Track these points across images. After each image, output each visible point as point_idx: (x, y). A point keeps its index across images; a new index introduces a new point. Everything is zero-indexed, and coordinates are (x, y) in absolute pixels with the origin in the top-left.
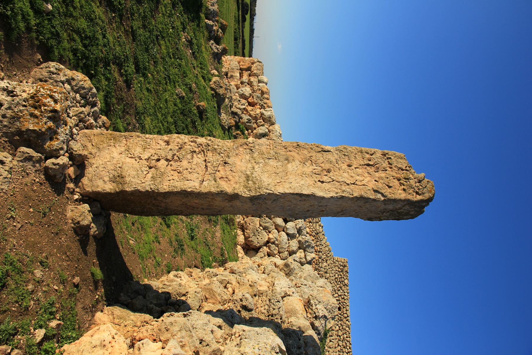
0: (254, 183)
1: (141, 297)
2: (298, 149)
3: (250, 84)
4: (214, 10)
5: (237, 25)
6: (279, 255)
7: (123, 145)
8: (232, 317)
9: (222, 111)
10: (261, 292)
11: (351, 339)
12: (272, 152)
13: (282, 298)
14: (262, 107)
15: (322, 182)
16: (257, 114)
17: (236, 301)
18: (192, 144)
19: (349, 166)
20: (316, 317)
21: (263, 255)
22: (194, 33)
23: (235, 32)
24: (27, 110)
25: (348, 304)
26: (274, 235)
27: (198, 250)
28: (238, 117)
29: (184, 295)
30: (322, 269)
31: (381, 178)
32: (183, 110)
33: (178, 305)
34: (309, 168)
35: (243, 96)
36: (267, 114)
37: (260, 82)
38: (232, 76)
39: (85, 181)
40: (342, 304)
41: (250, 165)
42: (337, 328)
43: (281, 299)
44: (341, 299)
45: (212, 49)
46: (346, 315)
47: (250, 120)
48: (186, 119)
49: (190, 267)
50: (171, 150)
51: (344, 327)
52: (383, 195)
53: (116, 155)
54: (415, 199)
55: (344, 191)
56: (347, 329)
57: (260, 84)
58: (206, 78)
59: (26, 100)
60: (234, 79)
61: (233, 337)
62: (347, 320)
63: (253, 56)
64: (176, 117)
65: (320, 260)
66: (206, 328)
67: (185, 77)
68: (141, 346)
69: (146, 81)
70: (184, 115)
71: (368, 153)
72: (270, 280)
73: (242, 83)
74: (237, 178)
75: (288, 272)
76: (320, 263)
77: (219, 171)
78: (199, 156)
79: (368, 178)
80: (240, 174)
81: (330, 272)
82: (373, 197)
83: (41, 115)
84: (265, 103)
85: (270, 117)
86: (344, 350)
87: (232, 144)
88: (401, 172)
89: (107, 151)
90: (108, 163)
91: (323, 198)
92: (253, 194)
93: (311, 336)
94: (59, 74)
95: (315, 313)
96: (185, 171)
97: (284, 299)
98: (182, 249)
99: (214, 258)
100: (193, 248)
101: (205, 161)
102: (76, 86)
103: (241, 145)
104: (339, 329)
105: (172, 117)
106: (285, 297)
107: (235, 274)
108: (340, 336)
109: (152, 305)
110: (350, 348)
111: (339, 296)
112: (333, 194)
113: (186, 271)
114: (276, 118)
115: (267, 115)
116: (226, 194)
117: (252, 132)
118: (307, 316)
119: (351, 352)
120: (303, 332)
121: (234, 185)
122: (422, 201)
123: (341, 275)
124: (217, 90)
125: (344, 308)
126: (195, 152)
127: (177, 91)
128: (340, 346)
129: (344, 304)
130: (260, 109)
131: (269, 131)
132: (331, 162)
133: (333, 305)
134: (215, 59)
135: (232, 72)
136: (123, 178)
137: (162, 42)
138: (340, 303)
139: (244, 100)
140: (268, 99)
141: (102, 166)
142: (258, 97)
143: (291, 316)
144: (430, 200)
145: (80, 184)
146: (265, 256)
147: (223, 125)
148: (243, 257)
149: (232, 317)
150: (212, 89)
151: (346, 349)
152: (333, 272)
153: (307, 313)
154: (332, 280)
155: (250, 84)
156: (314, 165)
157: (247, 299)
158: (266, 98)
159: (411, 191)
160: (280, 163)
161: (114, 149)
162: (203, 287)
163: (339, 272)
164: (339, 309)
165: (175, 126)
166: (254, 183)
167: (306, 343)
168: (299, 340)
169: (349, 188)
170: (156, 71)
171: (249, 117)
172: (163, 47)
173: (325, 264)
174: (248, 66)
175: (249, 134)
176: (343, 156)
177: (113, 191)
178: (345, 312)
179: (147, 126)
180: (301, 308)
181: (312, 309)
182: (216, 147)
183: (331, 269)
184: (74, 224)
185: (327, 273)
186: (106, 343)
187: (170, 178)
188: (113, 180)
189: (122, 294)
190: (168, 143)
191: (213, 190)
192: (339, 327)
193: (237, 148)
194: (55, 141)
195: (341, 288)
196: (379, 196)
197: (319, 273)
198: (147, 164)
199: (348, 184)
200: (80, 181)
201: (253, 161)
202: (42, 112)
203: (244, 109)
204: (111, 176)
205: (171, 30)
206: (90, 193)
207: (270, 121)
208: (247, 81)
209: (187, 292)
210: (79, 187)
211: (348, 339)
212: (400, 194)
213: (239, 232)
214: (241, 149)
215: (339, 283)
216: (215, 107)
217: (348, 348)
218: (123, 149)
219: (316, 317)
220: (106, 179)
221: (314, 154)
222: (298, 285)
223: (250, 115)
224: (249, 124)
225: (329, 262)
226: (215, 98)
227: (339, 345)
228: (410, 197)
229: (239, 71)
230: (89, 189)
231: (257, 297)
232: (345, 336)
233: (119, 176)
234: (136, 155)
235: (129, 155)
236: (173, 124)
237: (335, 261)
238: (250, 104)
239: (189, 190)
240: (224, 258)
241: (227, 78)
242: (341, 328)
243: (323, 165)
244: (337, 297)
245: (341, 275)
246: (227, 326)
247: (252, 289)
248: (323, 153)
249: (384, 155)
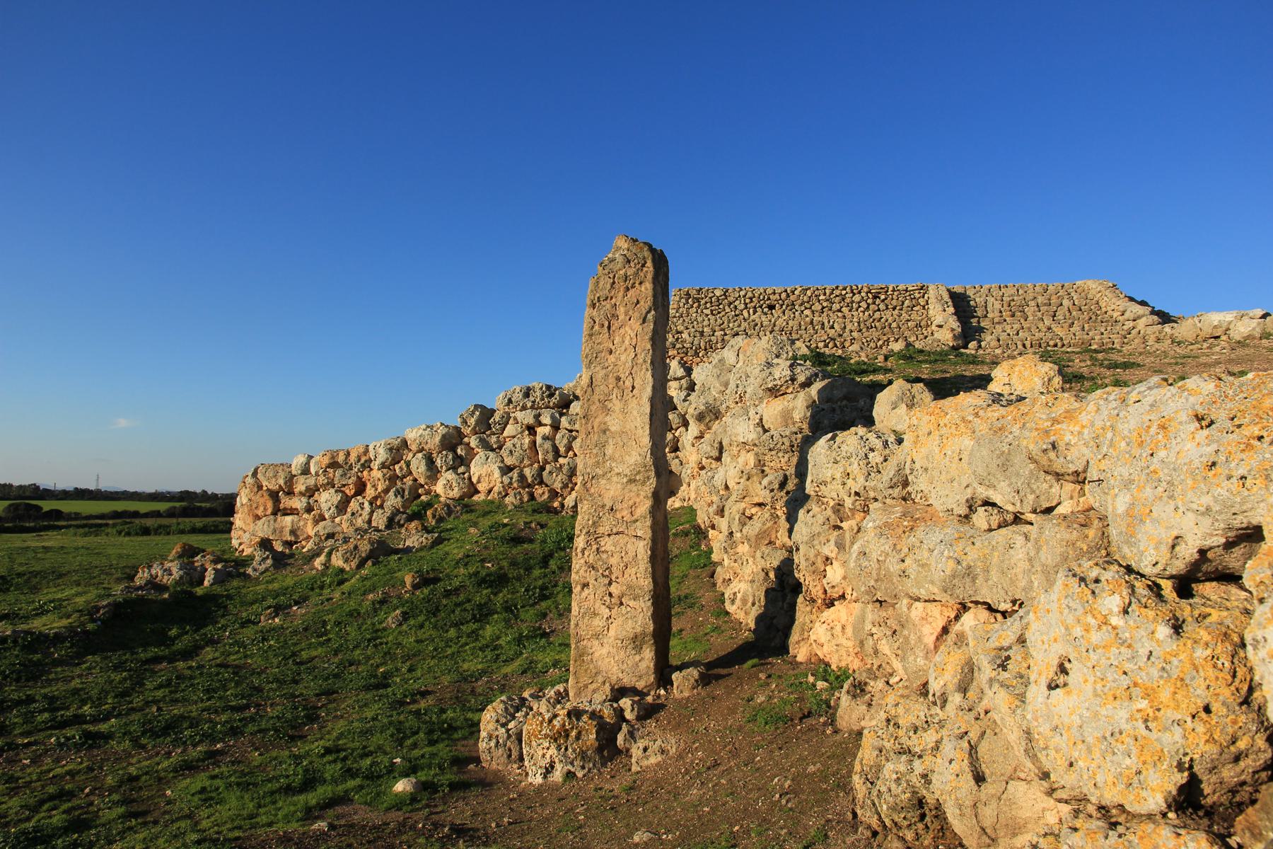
0: (639, 472)
1: (775, 621)
2: (589, 417)
3: (311, 492)
4: (181, 569)
5: (109, 530)
6: (676, 430)
7: (589, 644)
8: (796, 500)
9: (401, 546)
10: (757, 462)
11: (828, 287)
12: (595, 451)
13: (765, 431)
14: (367, 465)
15: (633, 387)
16: (384, 475)
17: (773, 498)
18: (586, 553)
19: (611, 352)
20: (793, 379)
21: (677, 460)
22: (252, 604)
23: (128, 534)
24: (572, 744)
25: (762, 291)
27: (681, 574)
28: (397, 515)
29: (767, 574)
30: (696, 342)
31: (626, 313)
32: (428, 612)
33: (782, 576)
34: (616, 405)
35: (342, 508)
36: (382, 455)
37: (306, 471)
38: (293, 532)
39: (640, 685)
40: (761, 302)
41: (615, 479)
42: (807, 312)
43: (768, 434)
44: (753, 304)
45: (267, 570)
46: (784, 295)
47: (397, 490)
48: (445, 606)
49: (714, 585)
50: (596, 580)
51: (806, 299)
52: (648, 312)
53: (604, 651)
54: (652, 269)
55: (645, 361)
56: (809, 293)
57: (313, 470)
58: (341, 577)
59: (559, 748)
60: (299, 528)
61: (819, 494)
62: (793, 292)
63: (218, 487)
64: (445, 624)
65: (678, 346)
66: (810, 523)
67: (359, 614)
68: (830, 585)
69: (396, 674)
70: (438, 610)
71: (593, 327)
72: (735, 450)
73: (309, 509)
74: (632, 494)
75: (711, 414)
76: (684, 347)
77: (623, 517)
78: (602, 544)
79: (627, 329)
80: (626, 491)
81: (700, 325)
82: (652, 324)
83: (577, 728)
84: (359, 461)
85: (391, 449)
86: (848, 300)
87: (586, 502)
88: (616, 286)
89: (600, 663)
90: (616, 659)
91: (653, 387)
92: (653, 474)
93: (819, 392)
94: (497, 736)
95: (787, 381)
96: (625, 560)
97: (766, 427)
98: (686, 597)
99: (692, 547)
100: (679, 583)
101: (609, 535)
102: (506, 717)
103: (587, 491)
104: (811, 308)
105: (447, 631)
106: (763, 426)
107: (723, 507)
108: (823, 308)
109: (785, 606)
110: (845, 289)
111: (746, 308)
112: (649, 374)
113: (722, 589)
114: (392, 438)
115: (385, 456)
116: (653, 507)
117: (422, 486)
118: (792, 393)
119: (851, 287)
120: (814, 401)
121: (642, 497)
122: (654, 261)
123: (706, 303)
124: (363, 555)
125: (769, 299)
126: (598, 549)
127: (393, 626)
128: (842, 307)
129: (761, 297)
130: (371, 469)
131: (421, 451)
132: (607, 375)
133: (771, 343)
134: (288, 564)
135: (281, 532)
136: (636, 637)
137: (305, 655)
138: (761, 307)
139: (351, 504)
140: (348, 454)
141: (620, 665)
142: (344, 475)
143: (792, 418)
144: (652, 250)
145: (645, 691)
146: (677, 457)
147: (433, 542)
148: (681, 499)
149: (796, 500)
150: (361, 565)
151: (847, 296)
152: (700, 319)
153: (786, 393)
154: (716, 320)
155: (311, 492)
156: (611, 397)
157: (771, 483)
158: (346, 458)
159: (642, 274)
160: (610, 441)
161: (596, 655)
162: (753, 550)
163: (699, 305)
164: (771, 307)
165: (462, 624)
166: (639, 472)
167: (829, 400)
168: (823, 410)
169: (641, 354)
170: (367, 662)
171: (391, 493)
172: (314, 653)
173: (685, 335)
174: (267, 497)
175: (428, 492)
176: (598, 359)
177: (654, 648)
178: (777, 296)
179: (480, 667)
180: (779, 402)
181: (781, 386)
182: (590, 522)
183: (695, 323)
184: (699, 685)
185: (703, 332)
186: (829, 627)
187: (634, 577)
188: (638, 649)
189: (773, 644)
190: (585, 585)
191: (649, 523)
192: (806, 308)
193: (591, 495)
194: (604, 713)
195: (731, 303)
196: (650, 316)
197: (703, 348)
198: (616, 608)
199: (636, 355)
200: (641, 691)
201: (609, 475)
202: (572, 728)
203: (371, 503)
204: (633, 652)
205: (272, 643)
206: (656, 676)
207: (398, 450)
208: (304, 500)
209: (763, 570)
210: (649, 691)
211: (828, 292)
212: (646, 289)
214: (592, 491)
215: (721, 307)
216: (400, 559)
217: (844, 292)
218: (596, 643)
219: (793, 379)
220: (637, 658)
221: (596, 397)
222: (737, 400)
223: (386, 491)
224: (406, 493)
225: (680, 328)
226: (380, 560)
227: (839, 311)
228: (650, 276)
229: (279, 518)
230: (652, 678)
231: (765, 468)
232: (822, 297)
233: (634, 642)
234: (605, 624)
235: (605, 632)
236: (460, 629)
237: (677, 315)
238: (361, 488)
239: (649, 552)
240: (692, 531)
241: (296, 543)
242: (808, 306)
243: (611, 386)
244: (749, 312)
245: (706, 303)
246: (807, 504)
247: (753, 476)
248: (594, 385)
249: (594, 306)
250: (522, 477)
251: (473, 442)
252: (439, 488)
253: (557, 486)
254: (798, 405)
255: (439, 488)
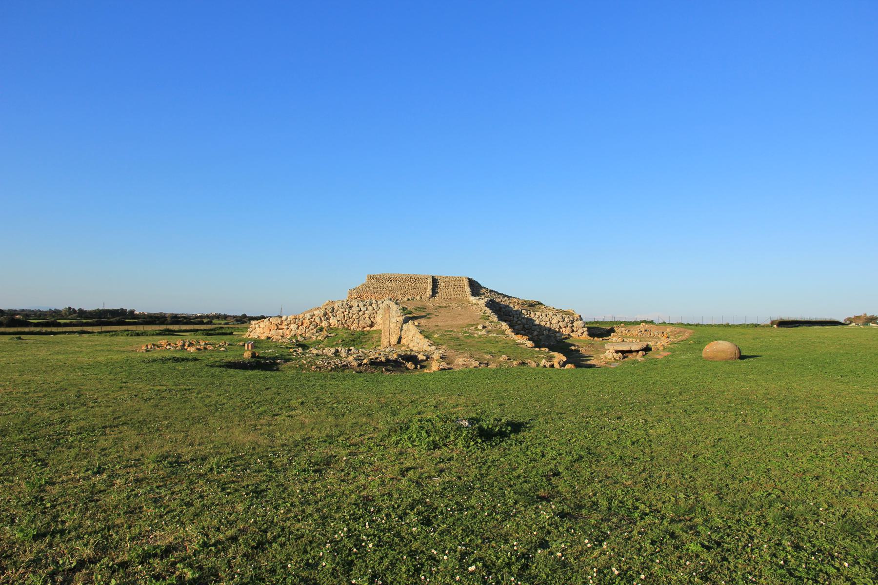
14: (304, 319)
23: (131, 335)
26: (367, 316)
35: (298, 328)
37: (286, 320)
57: (289, 319)
73: (288, 329)
164: (391, 281)
213: (365, 329)
223: (310, 325)
238: (302, 324)
250: (342, 323)
251: (330, 315)
252: (323, 324)
253: (350, 325)
254: (401, 319)
255: (323, 324)
